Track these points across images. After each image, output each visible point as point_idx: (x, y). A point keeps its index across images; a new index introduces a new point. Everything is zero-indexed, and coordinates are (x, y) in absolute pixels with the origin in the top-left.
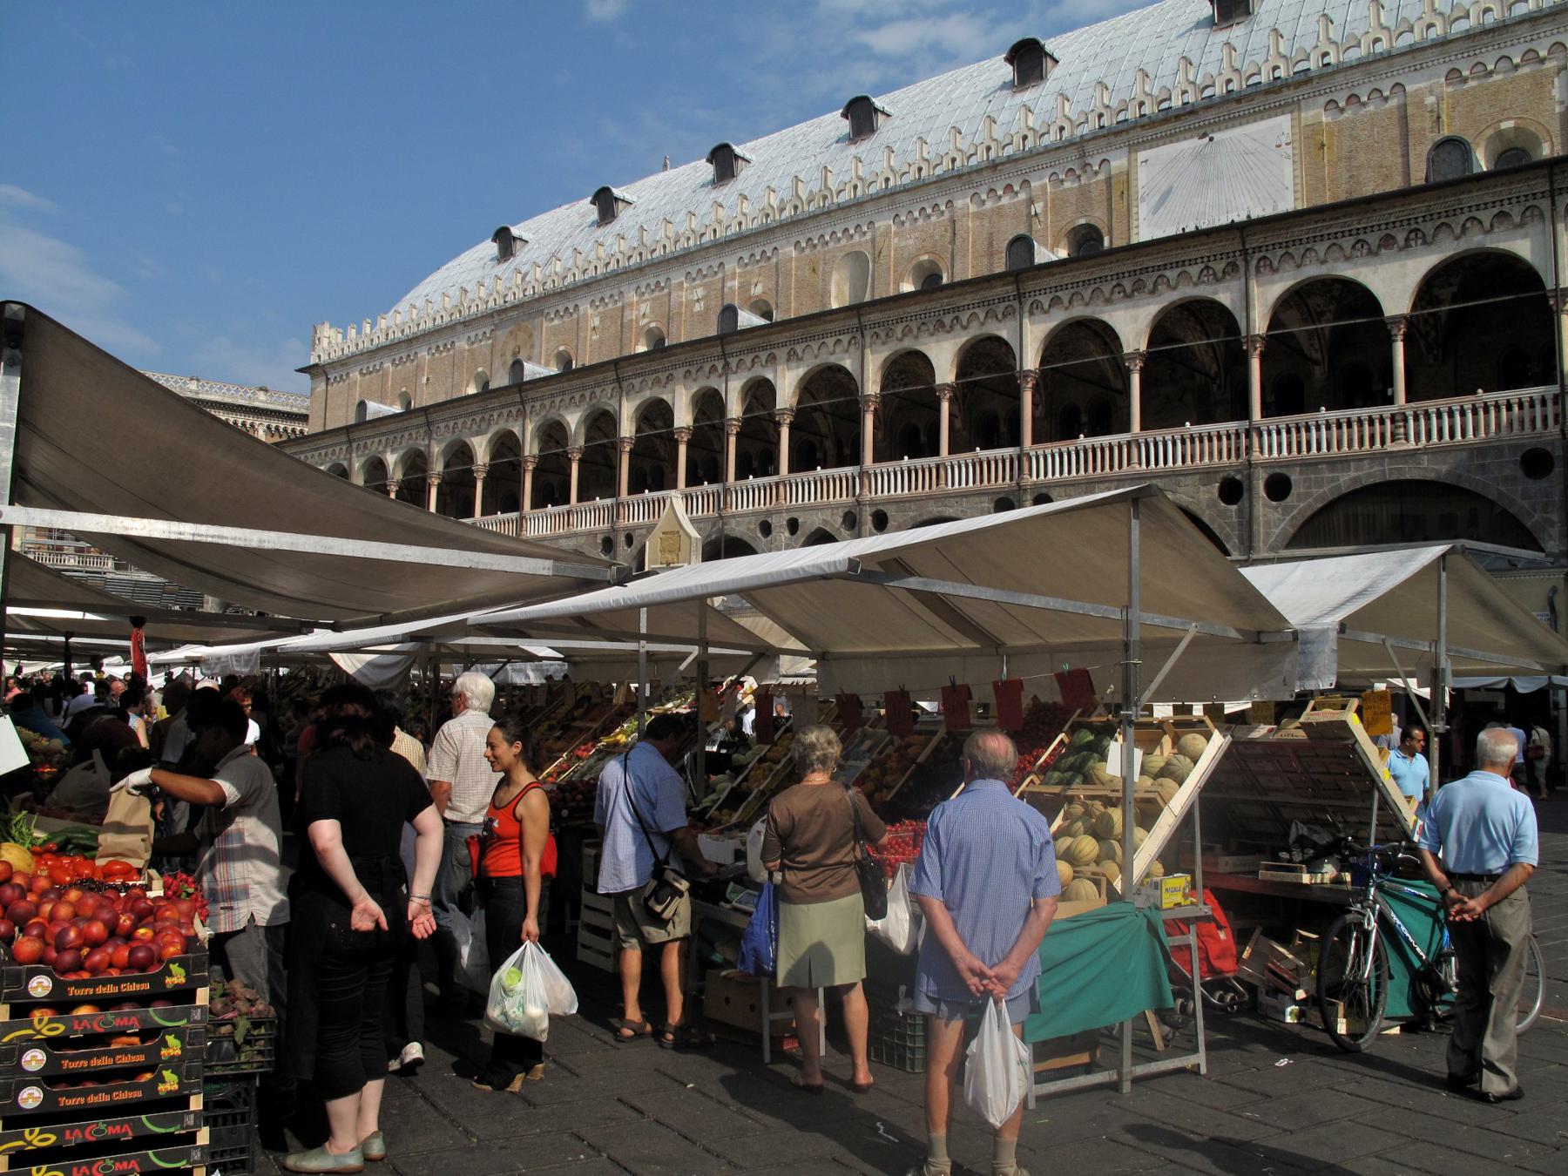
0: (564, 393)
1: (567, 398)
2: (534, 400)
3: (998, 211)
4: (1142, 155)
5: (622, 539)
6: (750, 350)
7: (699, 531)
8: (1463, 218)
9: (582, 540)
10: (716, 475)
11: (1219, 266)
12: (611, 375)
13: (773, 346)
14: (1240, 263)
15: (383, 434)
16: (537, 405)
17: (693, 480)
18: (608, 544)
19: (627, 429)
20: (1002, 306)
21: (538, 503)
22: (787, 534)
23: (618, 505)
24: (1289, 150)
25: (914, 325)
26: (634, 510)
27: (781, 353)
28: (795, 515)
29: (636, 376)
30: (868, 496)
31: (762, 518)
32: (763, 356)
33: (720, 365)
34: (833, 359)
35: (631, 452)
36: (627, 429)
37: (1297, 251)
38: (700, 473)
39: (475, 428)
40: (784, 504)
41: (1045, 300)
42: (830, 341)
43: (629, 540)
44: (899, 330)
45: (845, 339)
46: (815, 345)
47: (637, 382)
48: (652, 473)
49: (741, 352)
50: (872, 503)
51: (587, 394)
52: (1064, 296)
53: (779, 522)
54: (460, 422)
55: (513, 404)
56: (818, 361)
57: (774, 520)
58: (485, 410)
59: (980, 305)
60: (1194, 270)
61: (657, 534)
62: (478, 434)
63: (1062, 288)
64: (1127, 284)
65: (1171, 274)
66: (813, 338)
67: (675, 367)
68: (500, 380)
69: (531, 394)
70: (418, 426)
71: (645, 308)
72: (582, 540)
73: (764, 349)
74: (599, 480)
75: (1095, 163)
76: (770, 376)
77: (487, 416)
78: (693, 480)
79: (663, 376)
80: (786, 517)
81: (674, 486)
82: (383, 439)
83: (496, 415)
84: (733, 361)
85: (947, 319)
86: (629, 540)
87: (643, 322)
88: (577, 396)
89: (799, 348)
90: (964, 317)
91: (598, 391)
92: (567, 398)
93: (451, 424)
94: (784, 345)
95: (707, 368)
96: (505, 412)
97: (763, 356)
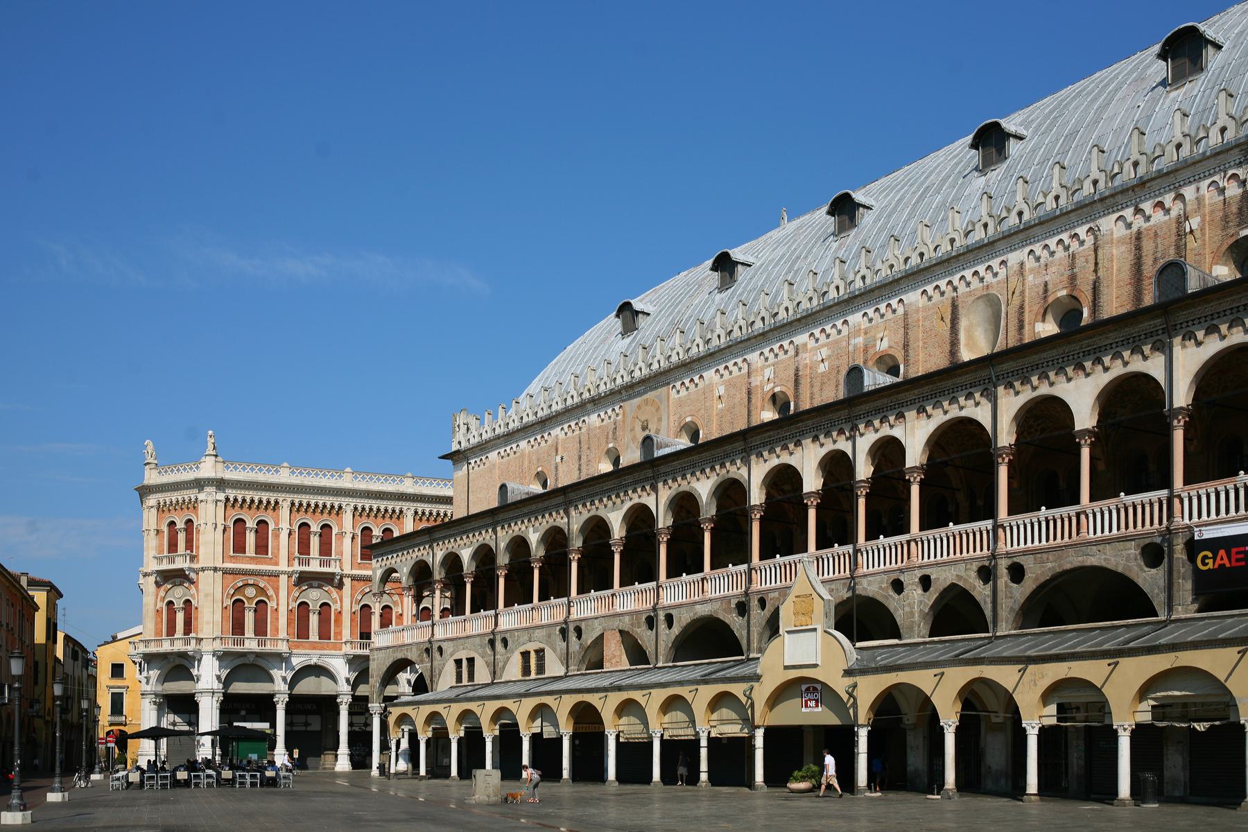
5: (754, 603)
7: (831, 591)
9: (716, 606)
10: (845, 535)
17: (822, 544)
18: (742, 608)
19: (757, 496)
21: (673, 573)
22: (920, 591)
23: (750, 570)
26: (766, 574)
28: (927, 571)
30: (1002, 547)
31: (894, 576)
35: (762, 519)
36: (757, 496)
38: (829, 533)
40: (917, 560)
43: (762, 603)
48: (783, 538)
50: (1008, 555)
53: (911, 581)
61: (791, 599)
68: (632, 456)
69: (663, 469)
71: (768, 373)
72: (716, 606)
74: (731, 549)
78: (822, 544)
80: (919, 573)
81: (805, 549)
86: (762, 603)
87: (768, 387)
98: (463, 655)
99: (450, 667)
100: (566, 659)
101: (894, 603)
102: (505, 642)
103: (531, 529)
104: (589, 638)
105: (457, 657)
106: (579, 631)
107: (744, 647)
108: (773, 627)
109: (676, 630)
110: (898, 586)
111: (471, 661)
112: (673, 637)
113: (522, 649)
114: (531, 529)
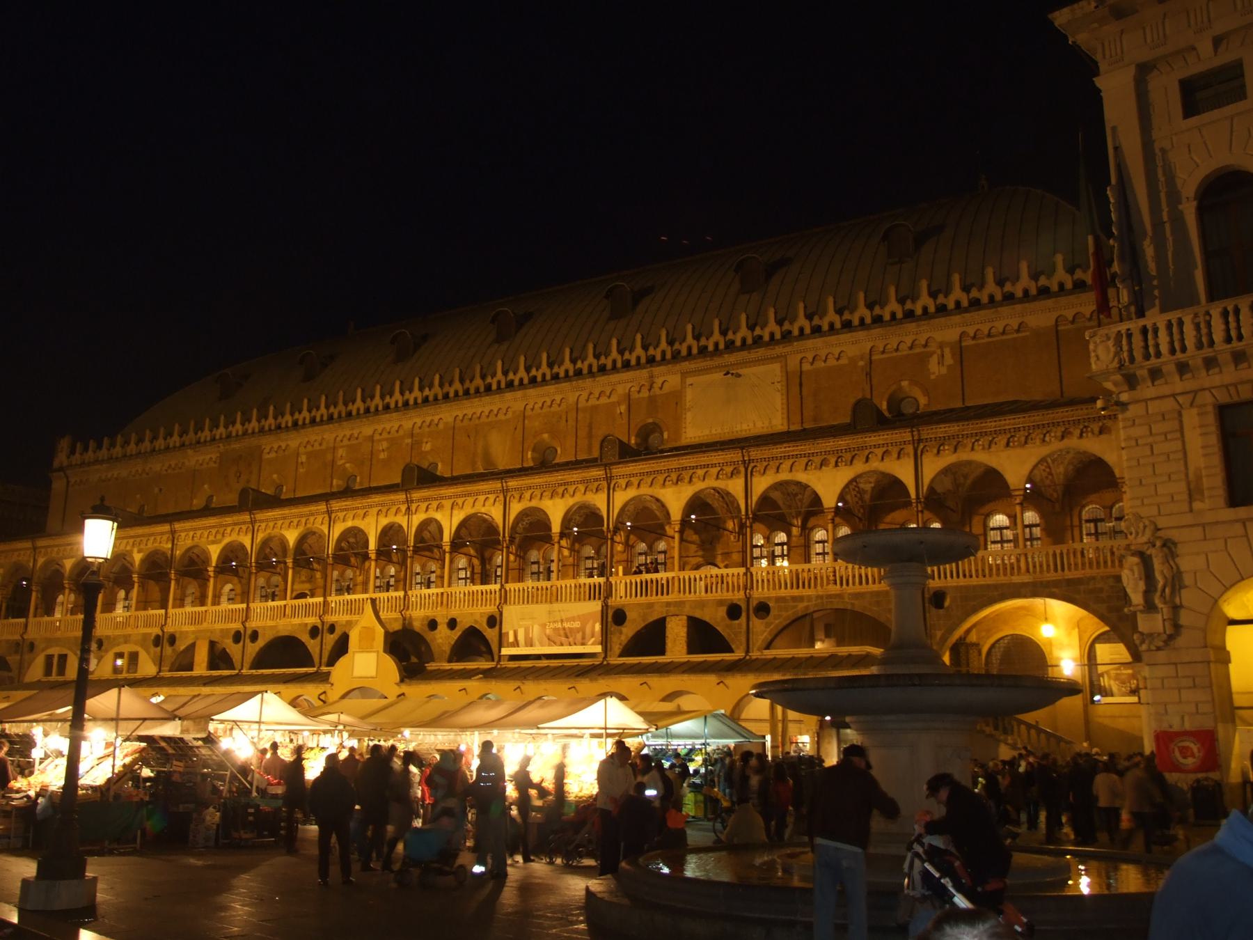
0: (285, 518)
1: (287, 522)
2: (261, 521)
3: (595, 408)
4: (689, 380)
6: (426, 499)
8: (867, 452)
11: (729, 469)
12: (322, 507)
13: (442, 498)
14: (742, 469)
15: (131, 537)
16: (263, 525)
20: (596, 484)
24: (779, 386)
25: (538, 493)
27: (447, 504)
29: (342, 510)
32: (435, 504)
33: (403, 508)
34: (483, 510)
37: (773, 464)
39: (211, 538)
41: (623, 482)
42: (482, 498)
44: (527, 495)
45: (492, 497)
46: (471, 500)
47: (341, 515)
49: (419, 500)
51: (303, 520)
52: (635, 481)
54: (199, 533)
55: (244, 523)
56: (472, 511)
57: (438, 620)
58: (221, 526)
59: (582, 482)
60: (714, 471)
62: (213, 542)
63: (633, 475)
64: (674, 476)
65: (701, 472)
66: (469, 495)
67: (371, 506)
70: (162, 534)
73: (436, 499)
75: (659, 381)
76: (438, 516)
77: (221, 530)
79: (361, 512)
82: (131, 541)
83: (229, 529)
84: (414, 507)
85: (560, 490)
88: (295, 521)
89: (460, 501)
90: (571, 489)
91: (312, 519)
92: (287, 522)
93: (191, 534)
94: (450, 497)
95: (394, 510)
96: (237, 528)
97: (435, 504)
98: (55, 651)
99: (40, 661)
100: (160, 662)
101: (429, 636)
102: (100, 643)
103: (135, 550)
104: (181, 646)
105: (50, 652)
106: (172, 640)
107: (316, 660)
108: (342, 647)
109: (261, 643)
110: (433, 625)
111: (63, 658)
112: (257, 649)
113: (117, 649)
114: (135, 550)
